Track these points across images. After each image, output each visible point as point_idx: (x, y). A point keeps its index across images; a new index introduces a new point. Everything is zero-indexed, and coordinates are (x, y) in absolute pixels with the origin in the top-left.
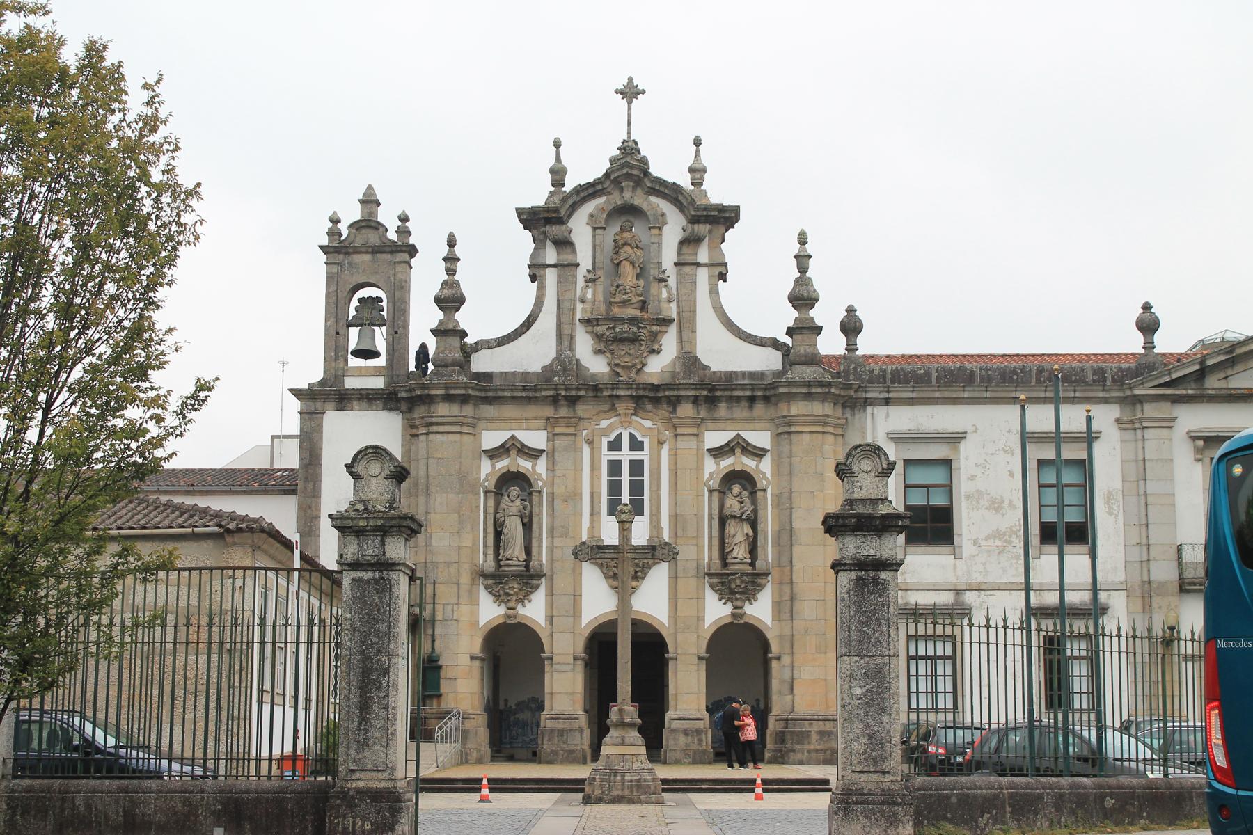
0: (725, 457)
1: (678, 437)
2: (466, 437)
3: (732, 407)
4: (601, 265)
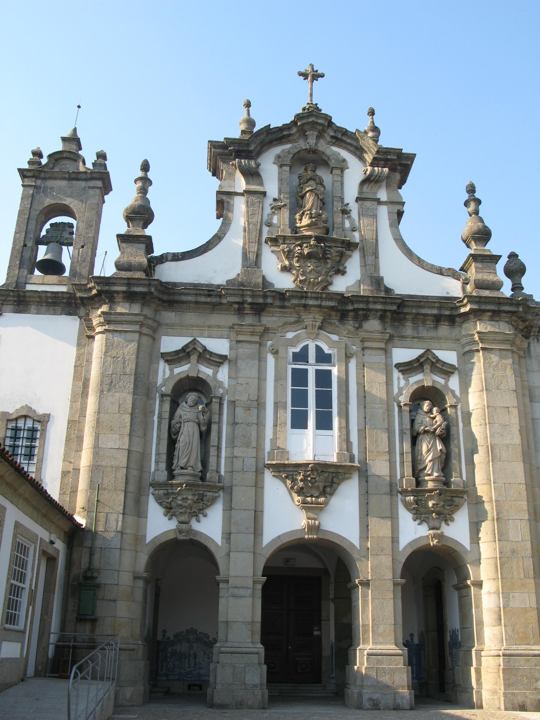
0: (414, 374)
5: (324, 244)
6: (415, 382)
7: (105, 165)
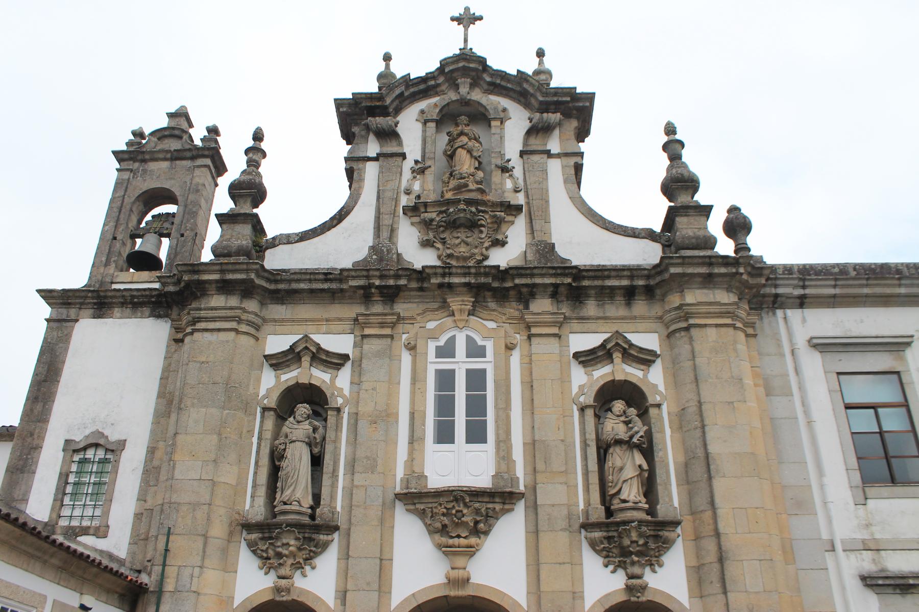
0: (599, 365)
1: (533, 339)
2: (244, 339)
3: (603, 305)
4: (432, 155)
5: (477, 209)
6: (601, 377)
7: (216, 142)
